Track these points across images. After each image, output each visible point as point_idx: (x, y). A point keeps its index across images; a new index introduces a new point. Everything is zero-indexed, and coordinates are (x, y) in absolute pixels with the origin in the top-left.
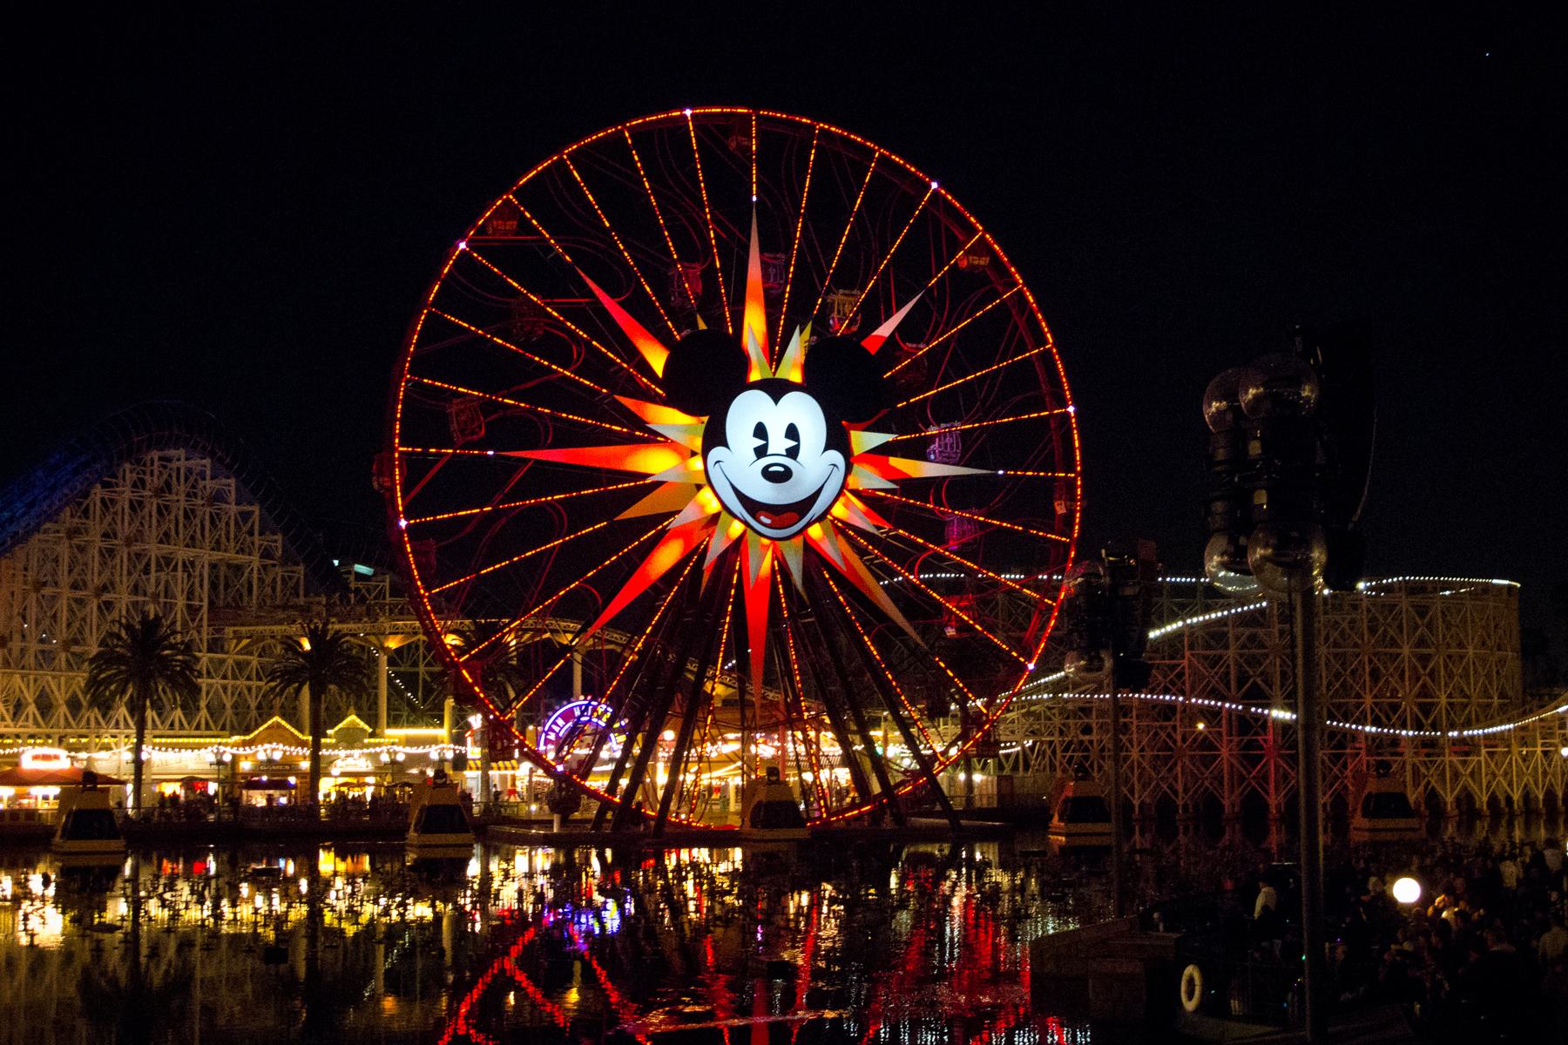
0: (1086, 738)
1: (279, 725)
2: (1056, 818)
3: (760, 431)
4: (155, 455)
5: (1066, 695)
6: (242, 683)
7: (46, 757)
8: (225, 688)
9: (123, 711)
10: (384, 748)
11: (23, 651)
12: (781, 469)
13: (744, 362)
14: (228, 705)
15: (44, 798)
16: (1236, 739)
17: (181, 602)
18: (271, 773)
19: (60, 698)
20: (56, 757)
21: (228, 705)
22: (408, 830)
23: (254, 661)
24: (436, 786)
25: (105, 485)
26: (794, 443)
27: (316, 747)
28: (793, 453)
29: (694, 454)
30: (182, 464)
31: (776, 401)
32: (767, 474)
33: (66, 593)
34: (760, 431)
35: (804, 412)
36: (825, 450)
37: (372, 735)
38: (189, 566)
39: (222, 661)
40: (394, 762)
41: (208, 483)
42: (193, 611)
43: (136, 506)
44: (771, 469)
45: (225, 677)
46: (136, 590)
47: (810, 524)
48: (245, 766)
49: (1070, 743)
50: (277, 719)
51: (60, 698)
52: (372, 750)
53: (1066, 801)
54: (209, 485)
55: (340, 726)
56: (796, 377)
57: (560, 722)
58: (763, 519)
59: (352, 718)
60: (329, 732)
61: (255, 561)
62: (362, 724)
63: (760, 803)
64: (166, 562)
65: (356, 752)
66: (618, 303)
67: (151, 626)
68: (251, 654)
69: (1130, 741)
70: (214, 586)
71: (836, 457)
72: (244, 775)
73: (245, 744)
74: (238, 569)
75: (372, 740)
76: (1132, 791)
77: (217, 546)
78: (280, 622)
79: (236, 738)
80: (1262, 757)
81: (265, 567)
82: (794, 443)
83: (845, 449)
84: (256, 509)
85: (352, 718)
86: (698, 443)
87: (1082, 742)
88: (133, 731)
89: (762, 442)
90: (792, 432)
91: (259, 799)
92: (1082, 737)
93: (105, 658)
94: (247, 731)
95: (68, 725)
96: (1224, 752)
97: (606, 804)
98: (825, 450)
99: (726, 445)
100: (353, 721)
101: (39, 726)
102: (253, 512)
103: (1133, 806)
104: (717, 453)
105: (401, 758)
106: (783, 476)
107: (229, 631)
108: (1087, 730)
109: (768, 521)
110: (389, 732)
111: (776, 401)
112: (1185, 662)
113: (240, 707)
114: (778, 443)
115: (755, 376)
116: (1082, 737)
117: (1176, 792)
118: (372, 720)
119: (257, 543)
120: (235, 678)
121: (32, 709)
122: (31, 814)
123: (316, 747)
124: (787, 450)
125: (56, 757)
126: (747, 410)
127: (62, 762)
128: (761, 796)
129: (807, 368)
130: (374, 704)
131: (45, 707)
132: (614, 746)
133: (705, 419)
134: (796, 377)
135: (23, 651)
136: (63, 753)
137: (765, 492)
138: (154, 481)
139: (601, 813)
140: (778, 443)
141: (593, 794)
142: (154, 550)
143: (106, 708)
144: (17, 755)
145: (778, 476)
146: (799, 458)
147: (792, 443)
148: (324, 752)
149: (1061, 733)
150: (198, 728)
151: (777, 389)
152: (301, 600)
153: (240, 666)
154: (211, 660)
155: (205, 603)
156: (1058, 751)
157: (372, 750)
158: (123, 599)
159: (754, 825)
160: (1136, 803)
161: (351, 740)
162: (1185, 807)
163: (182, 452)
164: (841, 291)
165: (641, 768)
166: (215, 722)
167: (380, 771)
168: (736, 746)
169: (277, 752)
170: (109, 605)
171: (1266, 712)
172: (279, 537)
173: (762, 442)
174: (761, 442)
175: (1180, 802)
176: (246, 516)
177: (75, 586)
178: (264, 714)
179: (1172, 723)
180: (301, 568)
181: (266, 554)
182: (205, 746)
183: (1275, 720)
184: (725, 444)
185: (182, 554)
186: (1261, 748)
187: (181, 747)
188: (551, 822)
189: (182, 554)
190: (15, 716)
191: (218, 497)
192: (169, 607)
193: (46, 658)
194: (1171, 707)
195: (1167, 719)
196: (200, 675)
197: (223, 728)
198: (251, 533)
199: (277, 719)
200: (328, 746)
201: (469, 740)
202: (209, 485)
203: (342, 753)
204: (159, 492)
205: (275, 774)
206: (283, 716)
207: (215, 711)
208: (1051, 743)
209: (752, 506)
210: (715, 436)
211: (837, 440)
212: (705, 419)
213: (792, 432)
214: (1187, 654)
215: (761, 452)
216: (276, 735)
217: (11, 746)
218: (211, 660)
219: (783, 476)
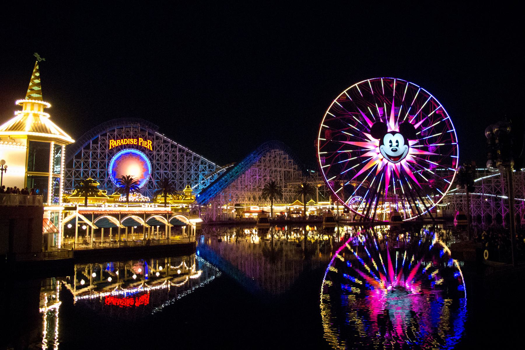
0: (461, 202)
1: (298, 202)
2: (455, 219)
3: (391, 142)
4: (273, 151)
5: (457, 194)
6: (291, 194)
7: (255, 208)
8: (287, 195)
9: (269, 199)
10: (318, 206)
11: (250, 188)
13: (386, 128)
14: (288, 198)
15: (255, 216)
16: (494, 202)
17: (279, 178)
18: (296, 211)
19: (257, 197)
20: (257, 208)
21: (288, 198)
22: (323, 221)
23: (293, 189)
24: (328, 213)
25: (264, 157)
26: (397, 144)
27: (305, 206)
28: (397, 146)
29: (377, 147)
30: (278, 152)
31: (394, 135)
32: (392, 150)
33: (258, 177)
34: (391, 142)
35: (400, 138)
36: (404, 145)
37: (316, 203)
38: (280, 171)
39: (287, 190)
40: (320, 209)
41: (283, 156)
42: (281, 180)
43: (270, 160)
45: (287, 193)
46: (270, 176)
47: (401, 160)
48: (292, 209)
49: (458, 203)
50: (297, 200)
51: (257, 197)
52: (316, 206)
53: (457, 215)
54: (283, 156)
55: (310, 202)
56: (397, 130)
57: (352, 201)
58: (392, 159)
59: (312, 200)
60: (307, 203)
61: (292, 170)
62: (314, 201)
63: (393, 216)
64: (276, 171)
65: (313, 207)
67: (273, 183)
68: (292, 188)
69: (471, 203)
70: (285, 175)
71: (406, 146)
72: (292, 211)
73: (291, 205)
74: (289, 172)
75: (316, 204)
76: (471, 213)
77: (285, 168)
78: (297, 182)
79: (290, 204)
80: (500, 206)
81: (294, 171)
82: (398, 144)
83: (408, 145)
84: (292, 160)
85: (312, 200)
86: (378, 145)
87: (460, 203)
88: (271, 203)
90: (397, 142)
91: (294, 216)
92: (460, 202)
93: (265, 189)
94: (292, 203)
95: (259, 202)
96: (492, 205)
97: (362, 217)
98: (404, 145)
99: (383, 144)
100: (312, 201)
101: (253, 202)
102: (291, 161)
103: (472, 217)
104: (382, 146)
105: (321, 208)
106: (396, 150)
107: (288, 184)
108: (461, 201)
109: (393, 160)
110: (319, 203)
111: (394, 135)
112: (482, 186)
113: (290, 198)
114: (394, 144)
115: (389, 130)
116: (460, 202)
117: (481, 214)
118: (316, 200)
119: (293, 167)
120: (289, 193)
121: (252, 199)
122: (253, 219)
123: (305, 206)
125: (257, 208)
126: (388, 138)
127: (258, 209)
128: (393, 215)
129: (400, 129)
130: (316, 197)
131: (254, 199)
132: (363, 205)
133: (380, 139)
134: (397, 130)
135: (250, 188)
136: (258, 207)
137: (392, 154)
138: (273, 156)
139: (361, 218)
140: (394, 144)
141: (359, 215)
142: (274, 169)
143: (265, 199)
144: (249, 208)
145: (395, 151)
147: (397, 144)
148: (306, 207)
149: (456, 201)
150: (283, 202)
151: (393, 133)
152: (301, 178)
153: (290, 190)
154: (285, 189)
155: (283, 179)
156: (455, 205)
157: (316, 206)
158: (268, 178)
159: (392, 221)
160: (473, 216)
161: (311, 204)
162: (483, 217)
163: (278, 150)
165: (369, 209)
166: (286, 201)
167: (317, 210)
168: (388, 205)
169: (298, 207)
170: (265, 179)
171: (501, 197)
172: (297, 166)
173: (391, 144)
174: (391, 144)
175: (482, 216)
176: (290, 162)
177: (259, 176)
178: (295, 200)
179: (480, 199)
180: (301, 172)
181: (294, 169)
182: (284, 206)
183: (503, 199)
184: (383, 144)
185: (279, 169)
186: (500, 204)
187: (280, 206)
188: (351, 220)
189: (279, 169)
190: (249, 200)
191: (285, 158)
192: (277, 179)
193: (254, 189)
194: (480, 196)
195: (479, 198)
196: (283, 192)
197: (287, 202)
198: (291, 165)
199: (297, 200)
200: (307, 206)
201: (334, 204)
202: (283, 156)
203: (310, 207)
204: (274, 158)
205: (298, 211)
206: (299, 200)
207: (286, 199)
208: (454, 203)
209: (390, 157)
210: (381, 143)
211: (406, 143)
212: (380, 139)
213: (397, 142)
214: (483, 185)
215: (391, 146)
216: (297, 204)
217: (248, 206)
218: (285, 189)
219: (396, 150)
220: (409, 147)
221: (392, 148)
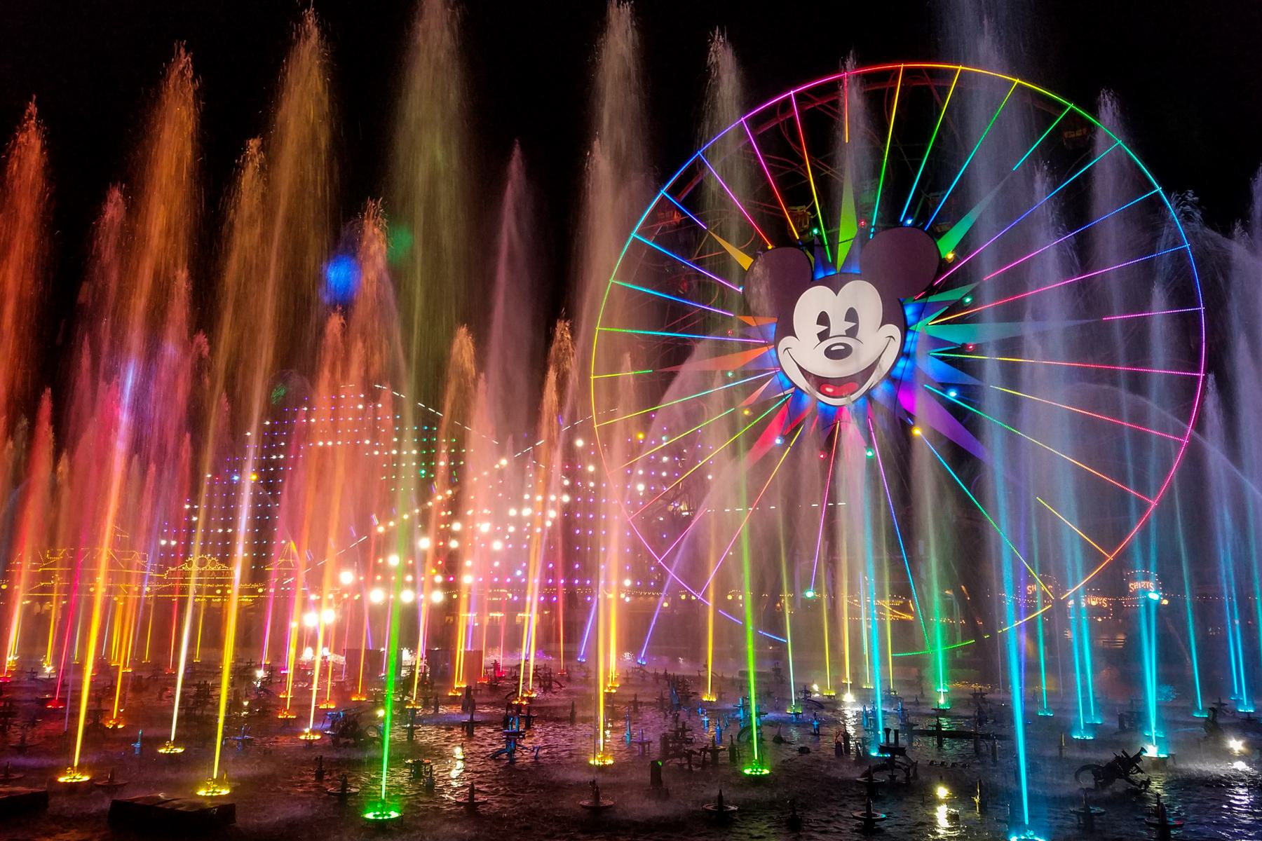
3: (823, 319)
12: (842, 347)
28: (852, 333)
32: (830, 353)
34: (823, 319)
36: (882, 324)
44: (833, 349)
66: (740, 250)
71: (894, 330)
89: (826, 328)
90: (852, 315)
98: (882, 324)
104: (787, 341)
109: (829, 390)
114: (839, 326)
124: (846, 331)
140: (839, 326)
146: (859, 336)
164: (932, 194)
210: (786, 328)
211: (894, 314)
213: (852, 315)
215: (823, 336)
220: (905, 329)
221: (827, 343)
